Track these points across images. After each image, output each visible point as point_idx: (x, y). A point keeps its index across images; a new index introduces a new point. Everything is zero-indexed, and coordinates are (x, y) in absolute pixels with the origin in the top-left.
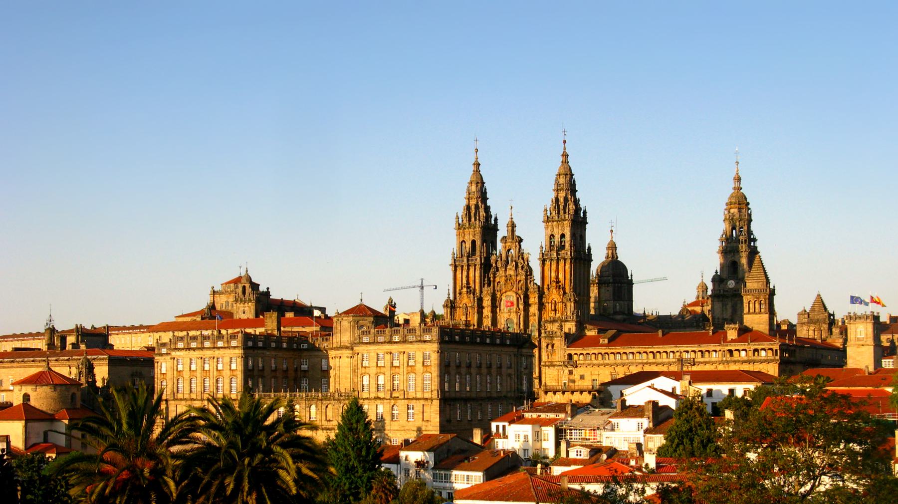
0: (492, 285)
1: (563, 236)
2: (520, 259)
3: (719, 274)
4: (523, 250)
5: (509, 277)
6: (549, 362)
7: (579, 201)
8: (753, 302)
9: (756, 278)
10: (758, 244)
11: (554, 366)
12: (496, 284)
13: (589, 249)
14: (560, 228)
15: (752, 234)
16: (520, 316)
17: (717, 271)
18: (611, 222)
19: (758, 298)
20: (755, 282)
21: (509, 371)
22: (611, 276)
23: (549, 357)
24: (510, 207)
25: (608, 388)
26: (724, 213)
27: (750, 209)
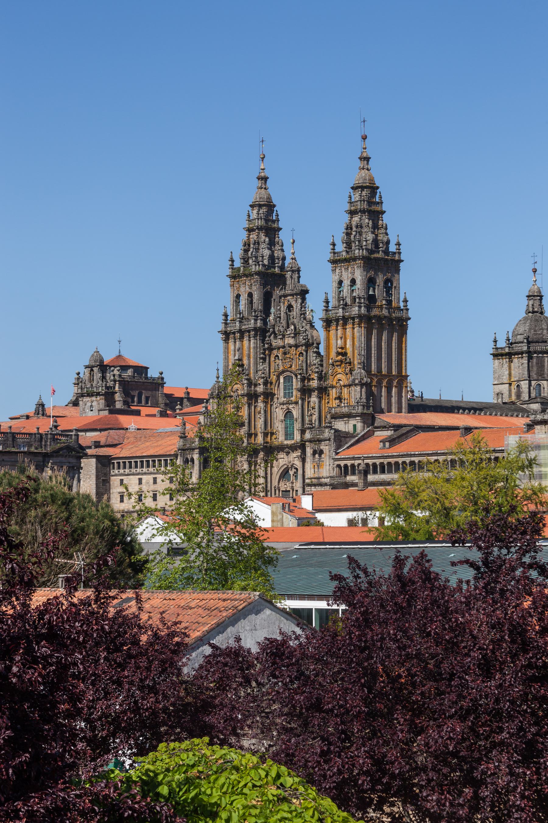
0: (267, 361)
1: (353, 282)
12: (272, 359)
13: (406, 301)
18: (534, 256)
22: (525, 341)
24: (291, 241)
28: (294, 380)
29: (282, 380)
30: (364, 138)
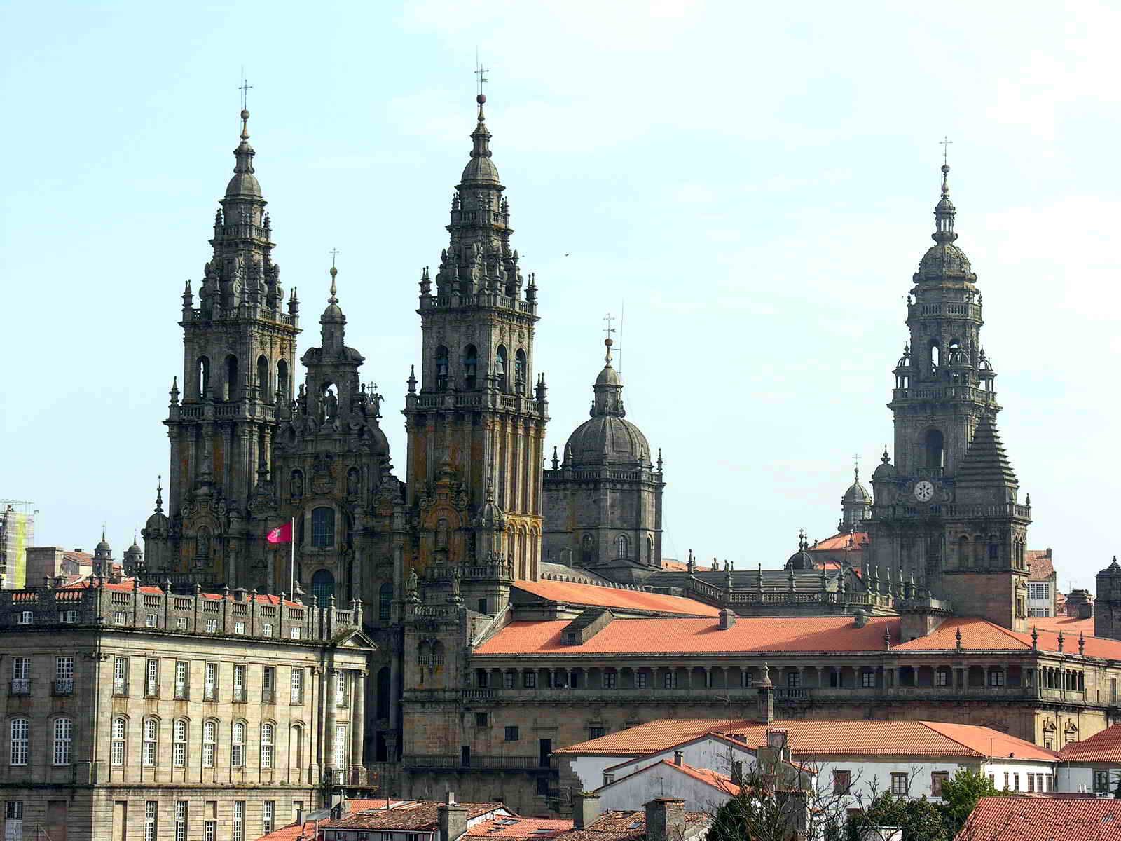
2: (356, 410)
3: (892, 462)
4: (363, 386)
5: (323, 456)
6: (422, 691)
7: (515, 259)
8: (971, 539)
9: (979, 478)
10: (998, 385)
11: (438, 702)
13: (541, 388)
14: (463, 329)
15: (982, 359)
16: (351, 563)
17: (886, 454)
19: (984, 530)
20: (976, 487)
21: (297, 713)
23: (425, 678)
25: (572, 764)
26: (909, 301)
27: (977, 292)
28: (338, 516)
29: (308, 516)
30: (481, 100)
